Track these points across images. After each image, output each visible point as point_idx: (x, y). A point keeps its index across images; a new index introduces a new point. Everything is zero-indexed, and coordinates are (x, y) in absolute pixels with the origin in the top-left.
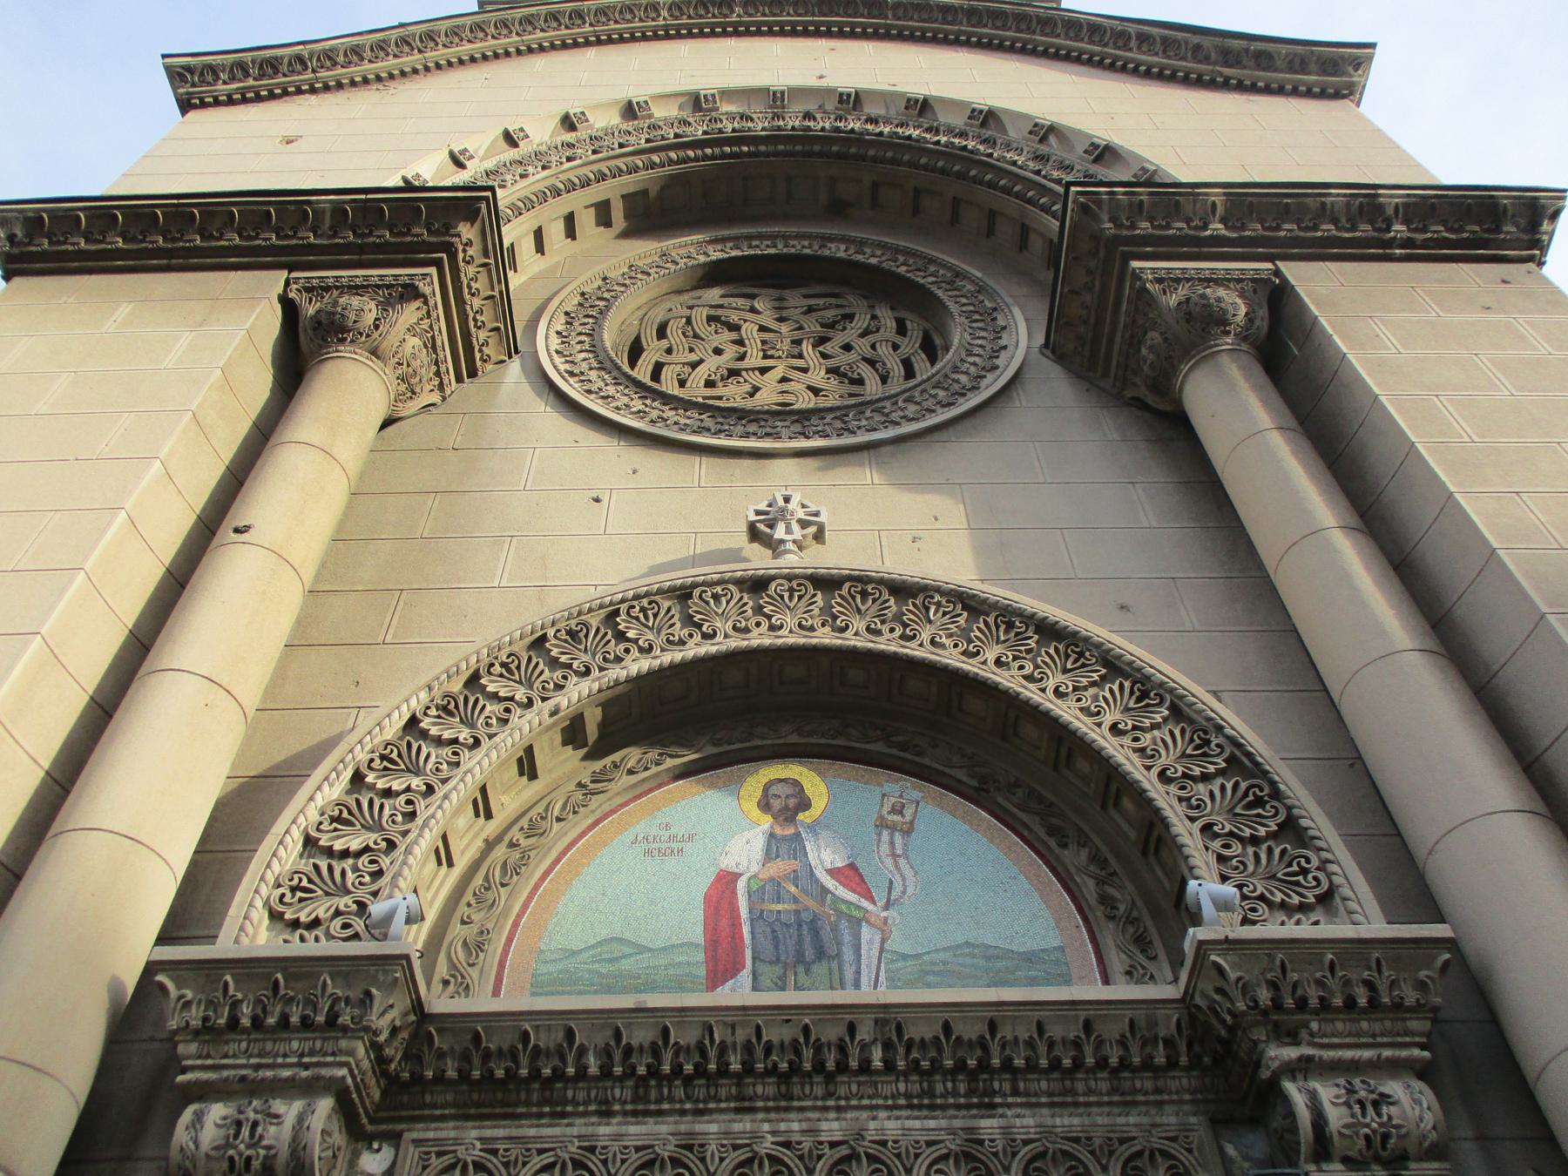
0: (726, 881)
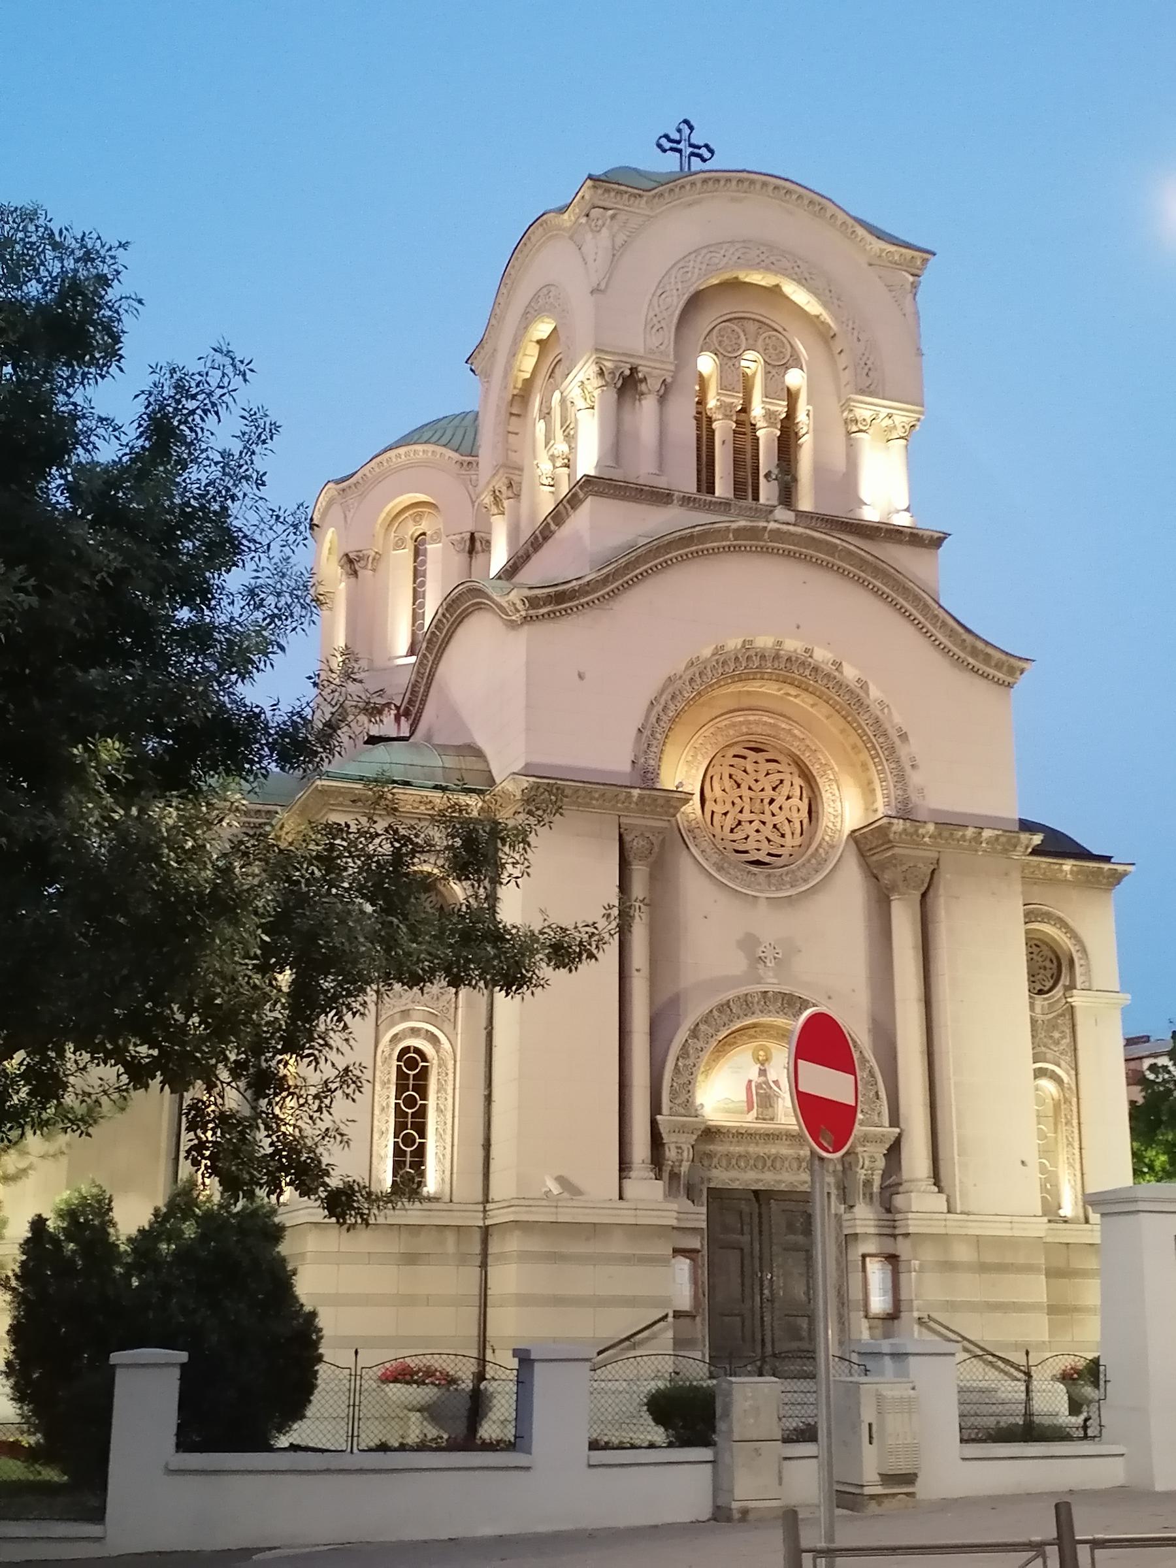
0: (750, 1081)
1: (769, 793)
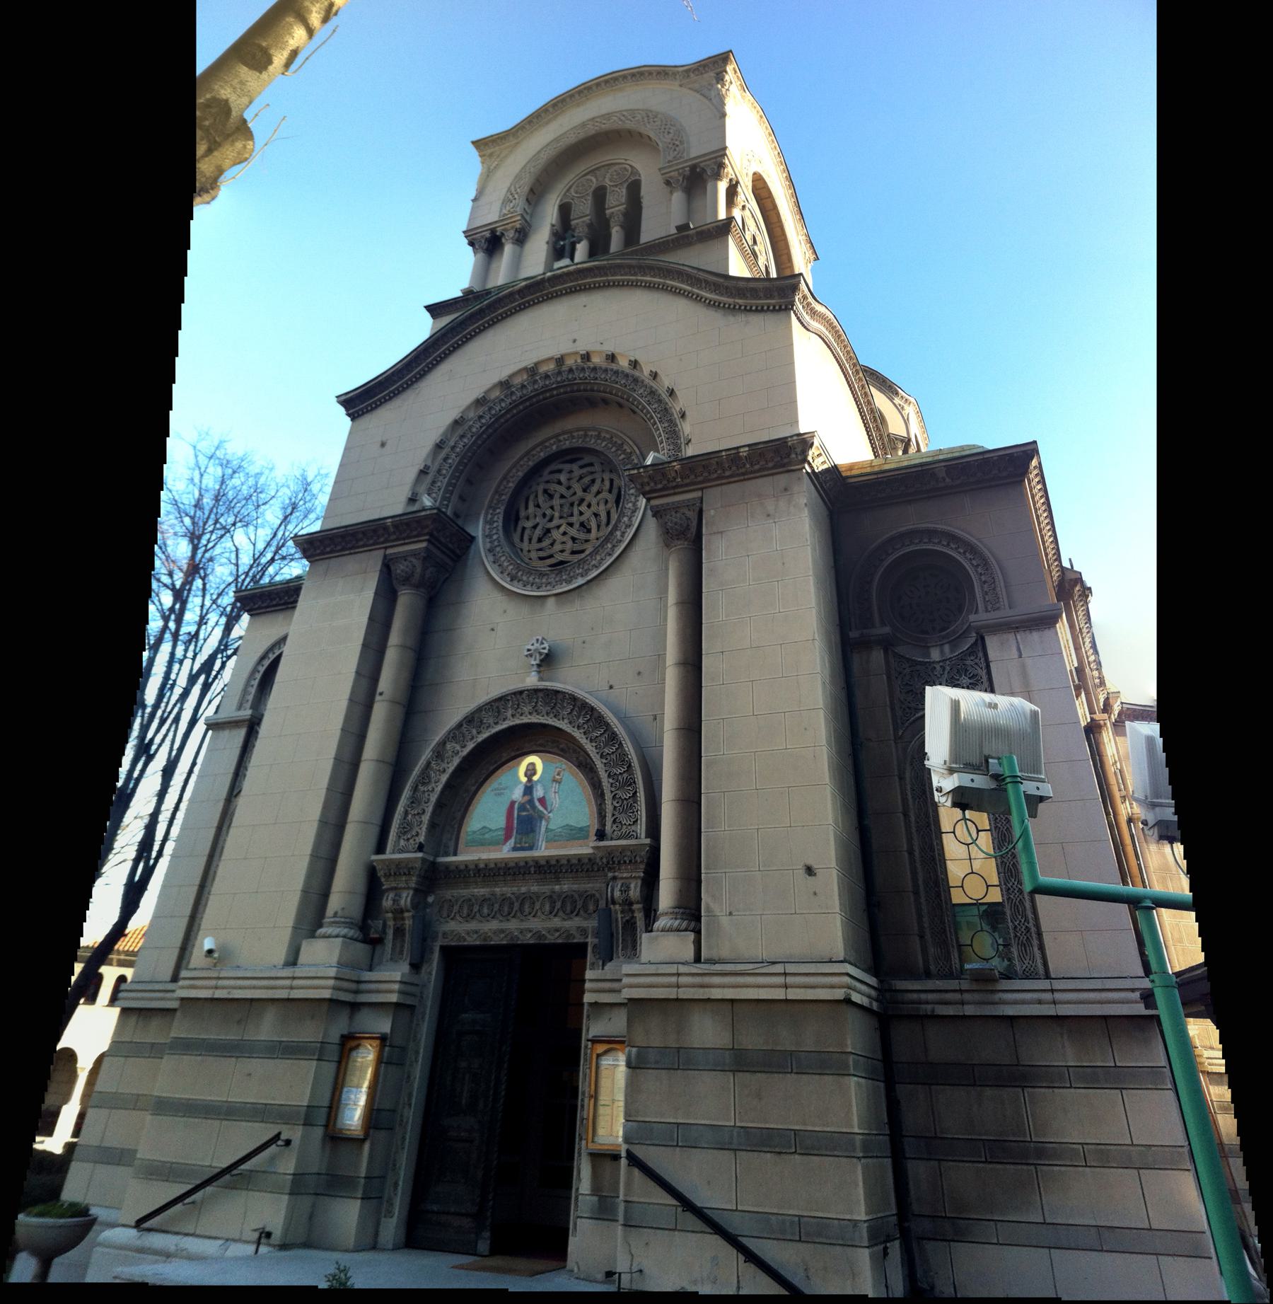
0: (513, 803)
1: (580, 493)
